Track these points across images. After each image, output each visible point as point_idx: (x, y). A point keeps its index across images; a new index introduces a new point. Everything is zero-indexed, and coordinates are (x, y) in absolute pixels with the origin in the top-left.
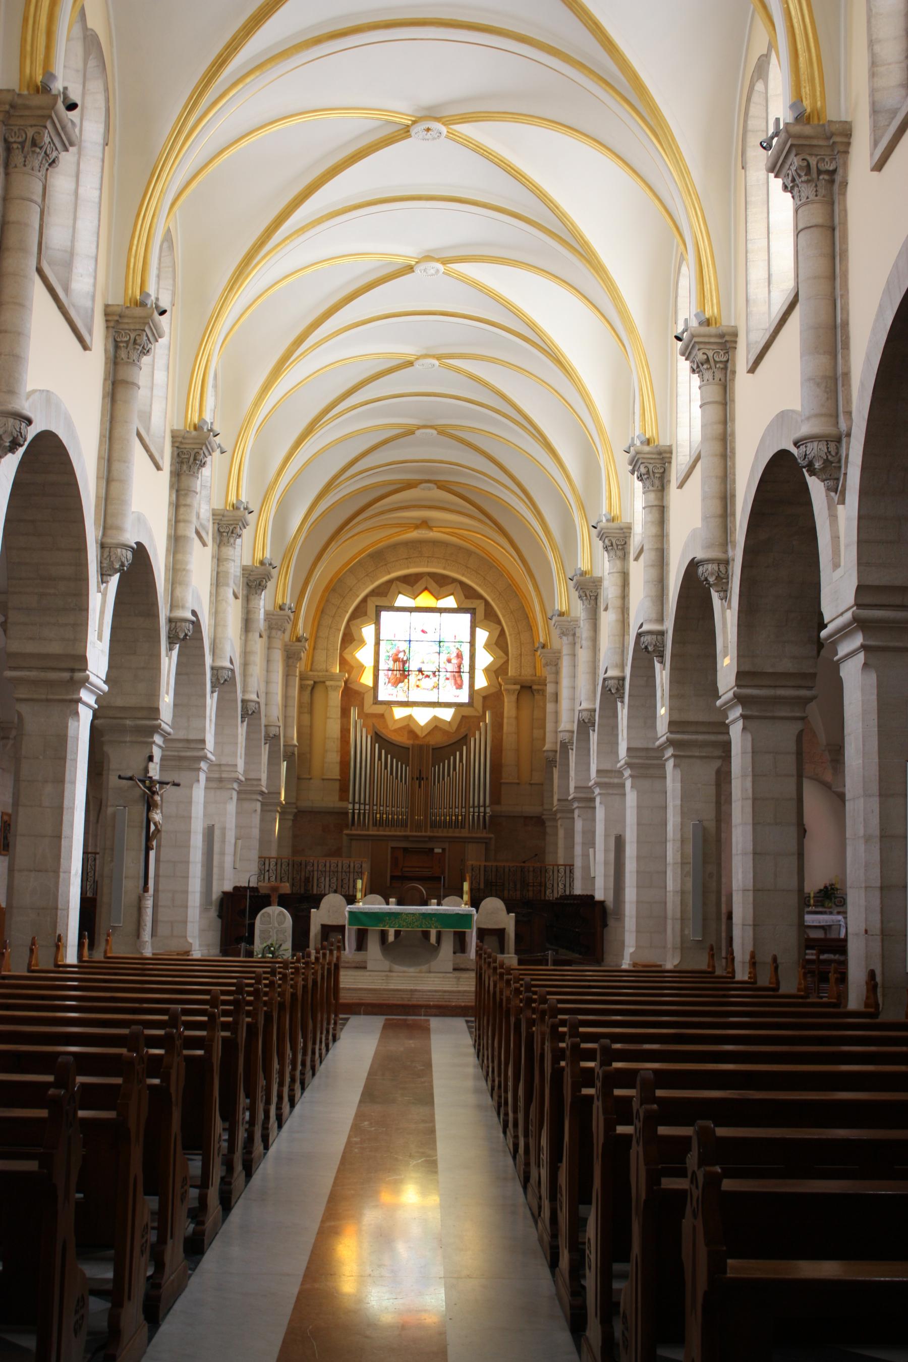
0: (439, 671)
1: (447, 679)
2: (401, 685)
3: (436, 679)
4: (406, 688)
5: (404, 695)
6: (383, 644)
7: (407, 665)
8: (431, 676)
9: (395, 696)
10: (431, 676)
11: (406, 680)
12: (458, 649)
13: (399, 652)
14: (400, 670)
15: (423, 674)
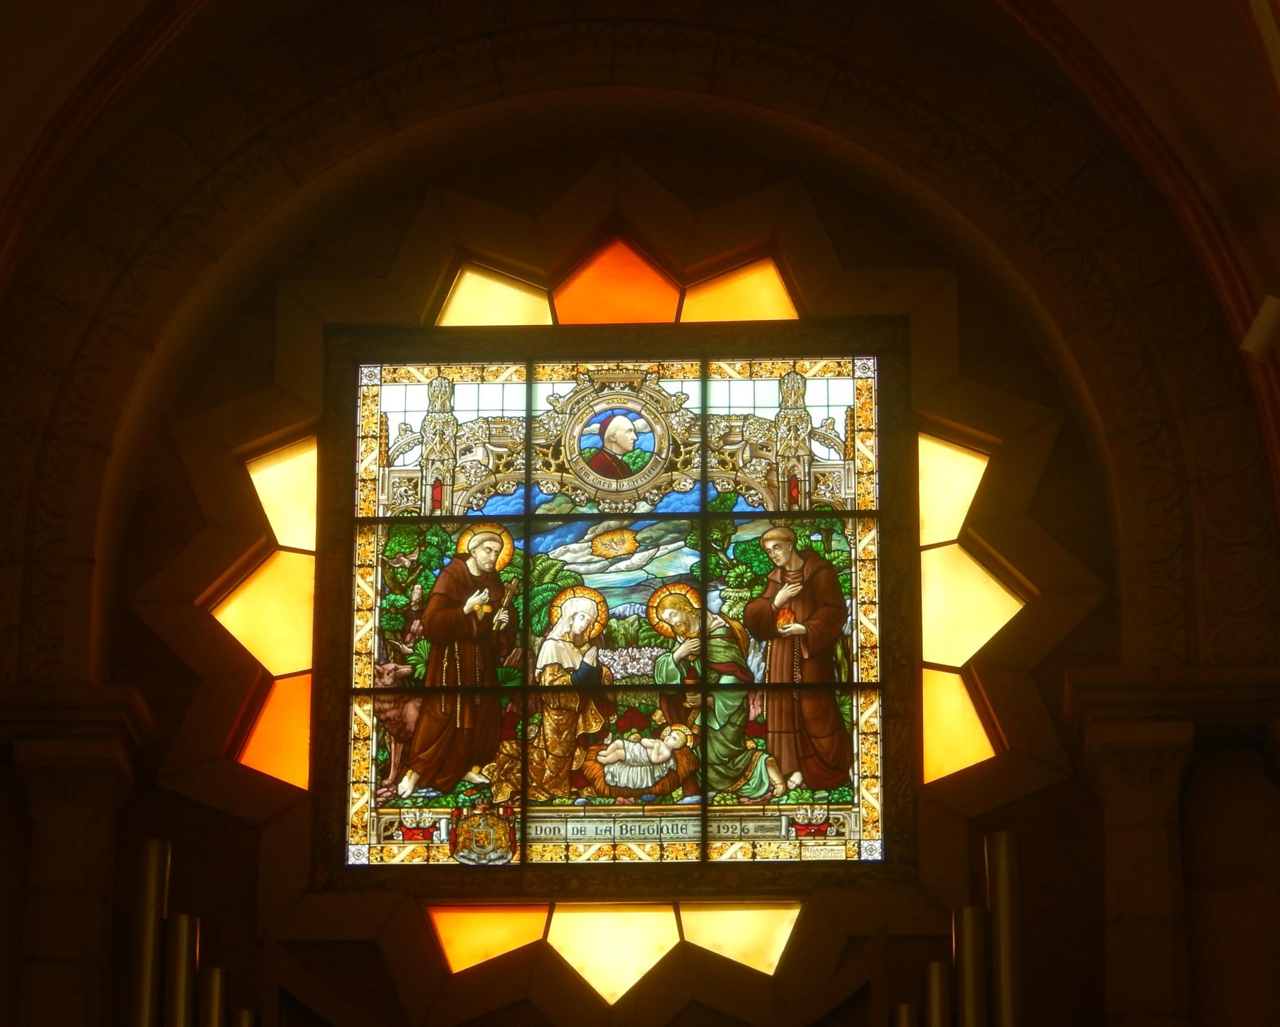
0: (706, 687)
1: (751, 729)
2: (475, 776)
3: (676, 737)
4: (503, 795)
5: (498, 833)
6: (367, 548)
7: (516, 653)
8: (658, 716)
9: (442, 833)
10: (658, 716)
11: (508, 747)
12: (808, 554)
13: (472, 585)
14: (468, 692)
15: (606, 708)
